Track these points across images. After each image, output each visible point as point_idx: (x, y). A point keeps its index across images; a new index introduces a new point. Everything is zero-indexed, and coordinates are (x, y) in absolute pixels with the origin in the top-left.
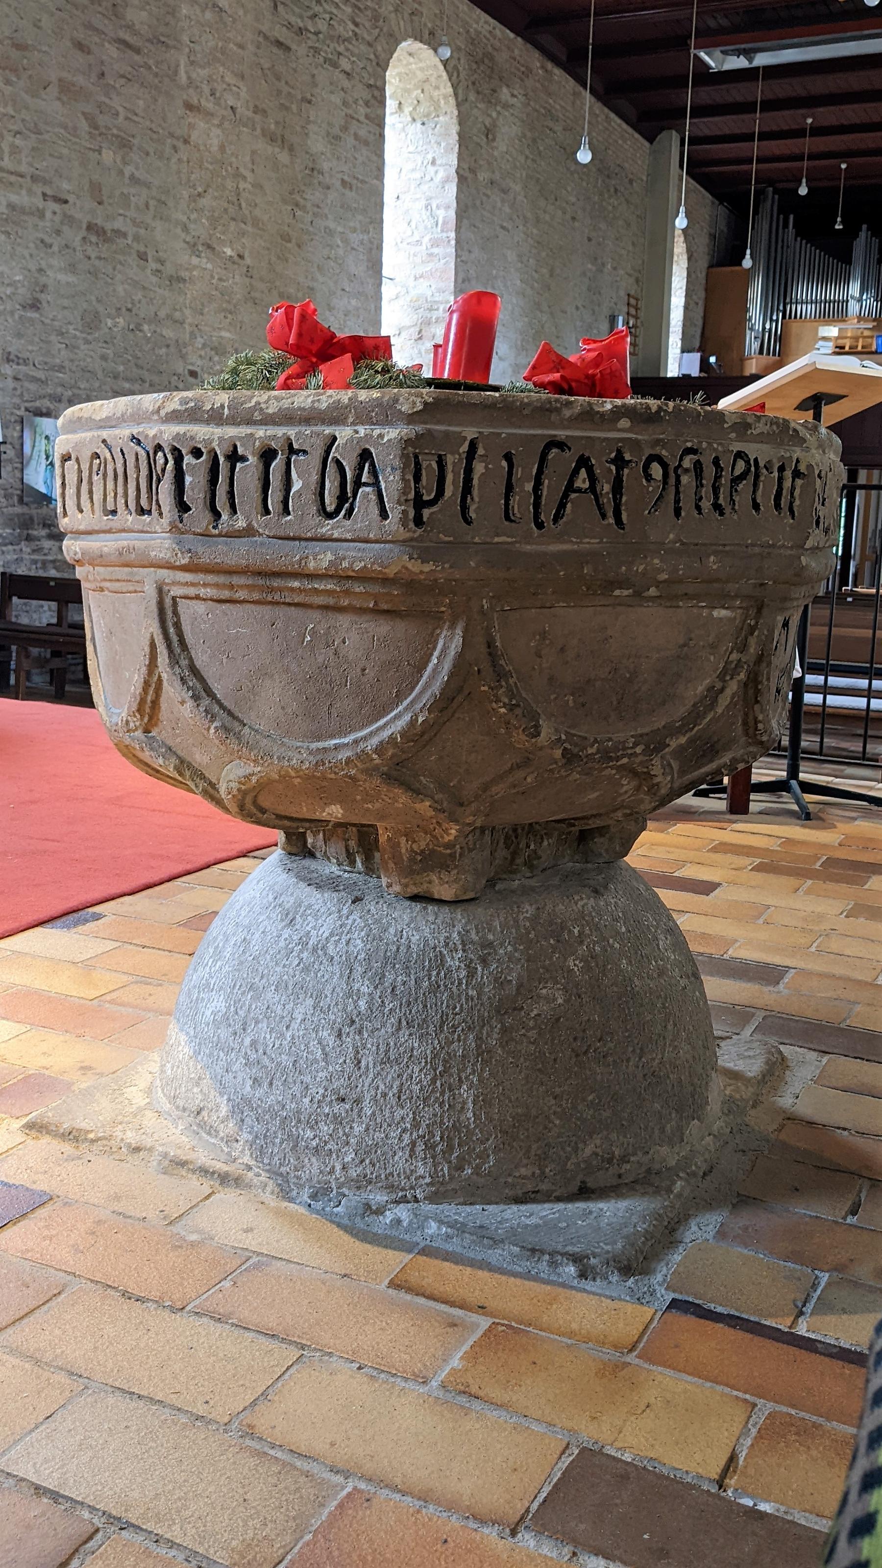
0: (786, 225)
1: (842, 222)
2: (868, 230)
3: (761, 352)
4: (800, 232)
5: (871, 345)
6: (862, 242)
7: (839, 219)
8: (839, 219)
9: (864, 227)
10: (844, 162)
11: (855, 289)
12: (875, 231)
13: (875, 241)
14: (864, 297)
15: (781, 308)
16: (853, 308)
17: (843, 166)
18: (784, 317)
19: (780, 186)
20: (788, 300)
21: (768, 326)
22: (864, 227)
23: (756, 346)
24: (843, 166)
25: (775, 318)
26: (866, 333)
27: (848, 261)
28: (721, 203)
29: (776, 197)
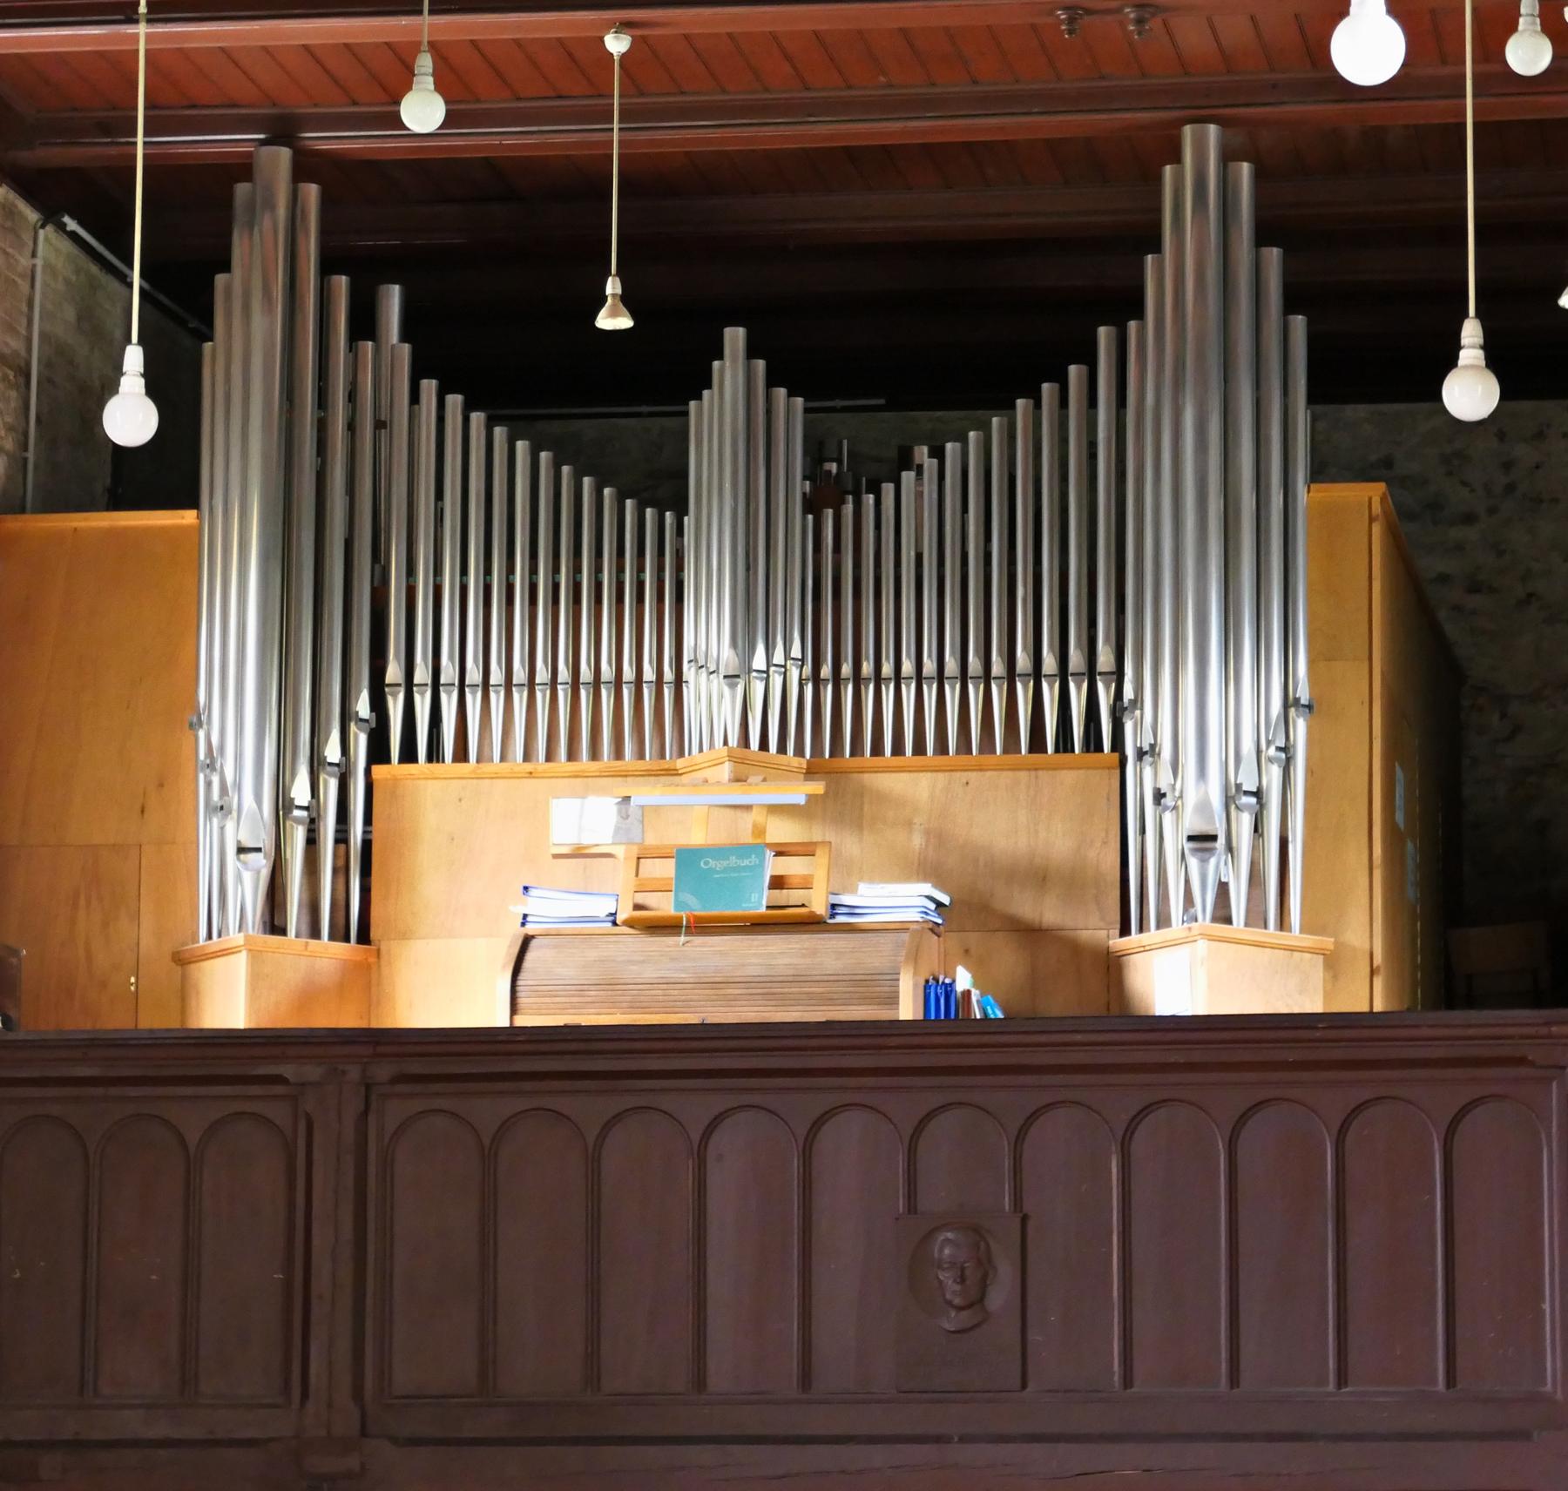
0: (364, 324)
1: (628, 300)
2: (752, 352)
3: (275, 925)
4: (441, 355)
5: (806, 885)
6: (730, 400)
7: (613, 287)
8: (613, 287)
9: (735, 337)
10: (624, 26)
11: (709, 630)
12: (785, 368)
13: (790, 408)
14: (759, 661)
15: (363, 707)
16: (712, 704)
17: (617, 44)
18: (379, 752)
19: (321, 140)
20: (394, 672)
21: (300, 792)
22: (735, 337)
23: (247, 887)
24: (617, 44)
25: (332, 752)
26: (782, 831)
27: (666, 489)
28: (51, 216)
29: (312, 192)
